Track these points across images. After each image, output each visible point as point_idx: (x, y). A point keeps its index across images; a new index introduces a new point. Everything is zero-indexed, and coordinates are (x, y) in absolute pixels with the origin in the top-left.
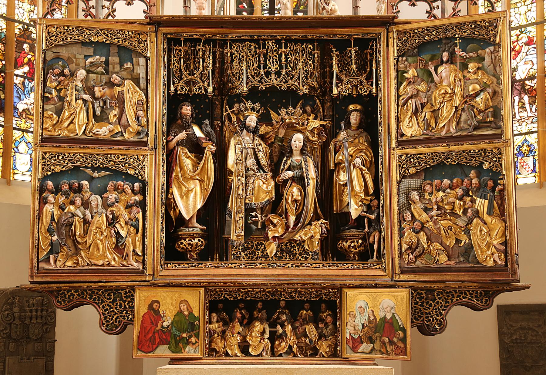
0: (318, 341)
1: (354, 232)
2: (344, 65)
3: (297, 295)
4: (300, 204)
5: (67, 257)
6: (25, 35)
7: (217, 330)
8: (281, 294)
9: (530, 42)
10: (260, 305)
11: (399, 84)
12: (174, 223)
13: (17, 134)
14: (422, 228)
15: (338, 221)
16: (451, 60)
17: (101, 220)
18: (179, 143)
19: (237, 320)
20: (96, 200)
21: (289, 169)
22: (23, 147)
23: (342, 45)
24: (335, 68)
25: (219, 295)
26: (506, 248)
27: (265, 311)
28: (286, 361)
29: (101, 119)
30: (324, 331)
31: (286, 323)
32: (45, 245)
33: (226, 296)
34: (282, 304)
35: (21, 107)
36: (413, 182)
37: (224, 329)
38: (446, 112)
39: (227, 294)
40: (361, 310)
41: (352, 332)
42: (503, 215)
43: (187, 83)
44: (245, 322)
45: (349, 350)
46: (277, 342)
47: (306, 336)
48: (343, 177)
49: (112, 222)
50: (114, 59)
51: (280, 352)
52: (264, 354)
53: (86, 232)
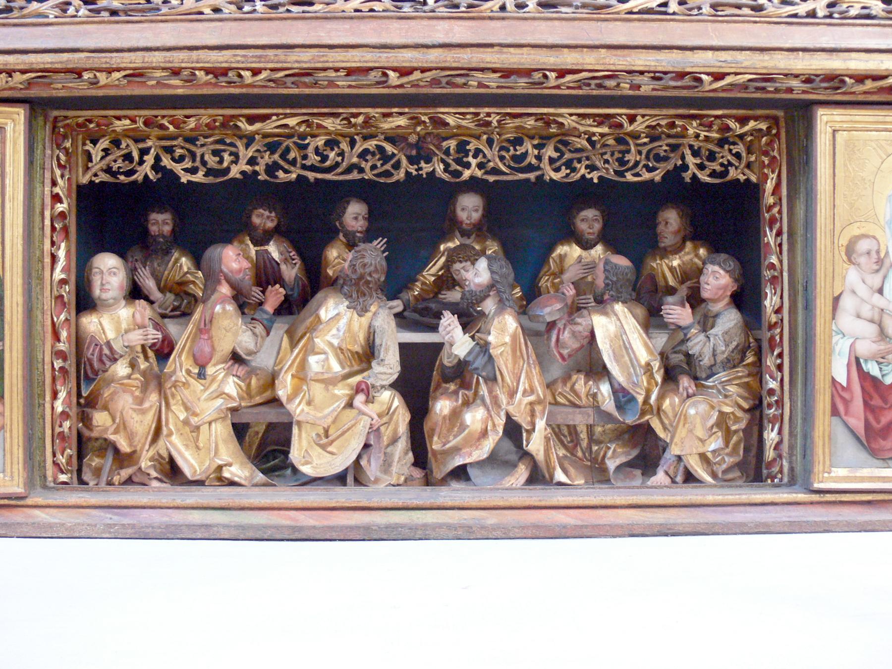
0: (661, 397)
3: (549, 152)
7: (117, 347)
8: (462, 147)
10: (354, 214)
19: (225, 289)
25: (128, 157)
27: (379, 244)
28: (491, 518)
30: (698, 344)
31: (489, 306)
33: (166, 162)
34: (469, 208)
37: (153, 335)
39: (169, 150)
41: (865, 348)
44: (275, 296)
45: (849, 449)
46: (442, 406)
47: (595, 368)
51: (458, 461)
52: (372, 468)
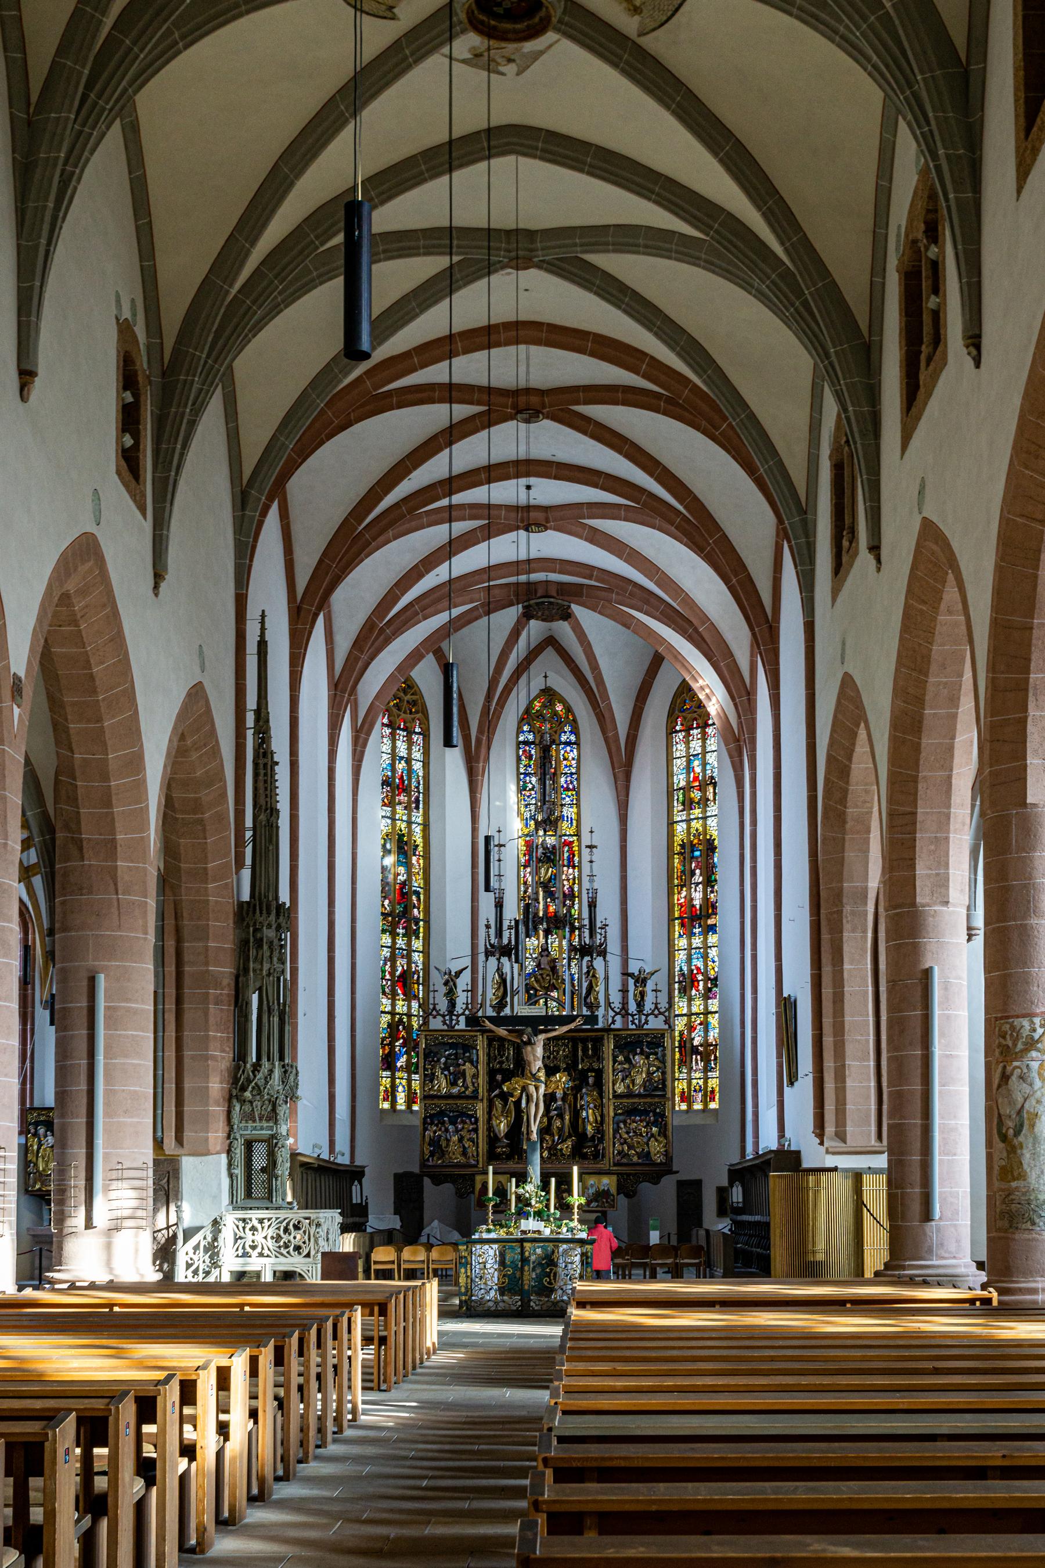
1: (590, 1144)
2: (585, 1050)
4: (560, 1130)
5: (439, 1159)
6: (401, 1020)
9: (701, 1024)
11: (614, 1063)
12: (493, 1139)
13: (398, 1081)
14: (625, 1142)
15: (581, 1138)
16: (642, 1053)
17: (455, 1138)
18: (495, 1096)
20: (451, 1128)
21: (555, 1110)
22: (400, 1089)
23: (584, 1040)
24: (580, 1053)
26: (666, 1154)
29: (454, 1084)
32: (427, 1152)
35: (399, 1064)
36: (621, 1118)
38: (639, 1080)
40: (592, 1186)
42: (666, 1137)
43: (499, 1063)
48: (584, 1114)
49: (461, 1140)
50: (460, 1051)
53: (448, 1145)
